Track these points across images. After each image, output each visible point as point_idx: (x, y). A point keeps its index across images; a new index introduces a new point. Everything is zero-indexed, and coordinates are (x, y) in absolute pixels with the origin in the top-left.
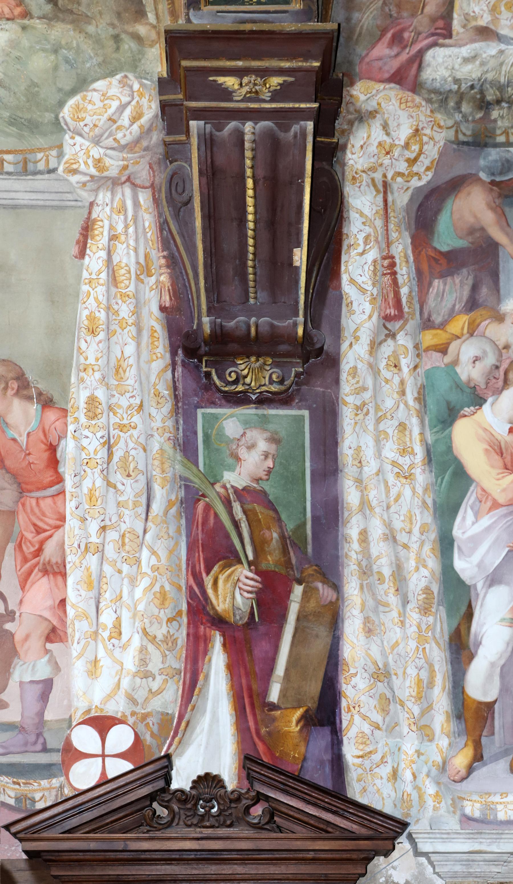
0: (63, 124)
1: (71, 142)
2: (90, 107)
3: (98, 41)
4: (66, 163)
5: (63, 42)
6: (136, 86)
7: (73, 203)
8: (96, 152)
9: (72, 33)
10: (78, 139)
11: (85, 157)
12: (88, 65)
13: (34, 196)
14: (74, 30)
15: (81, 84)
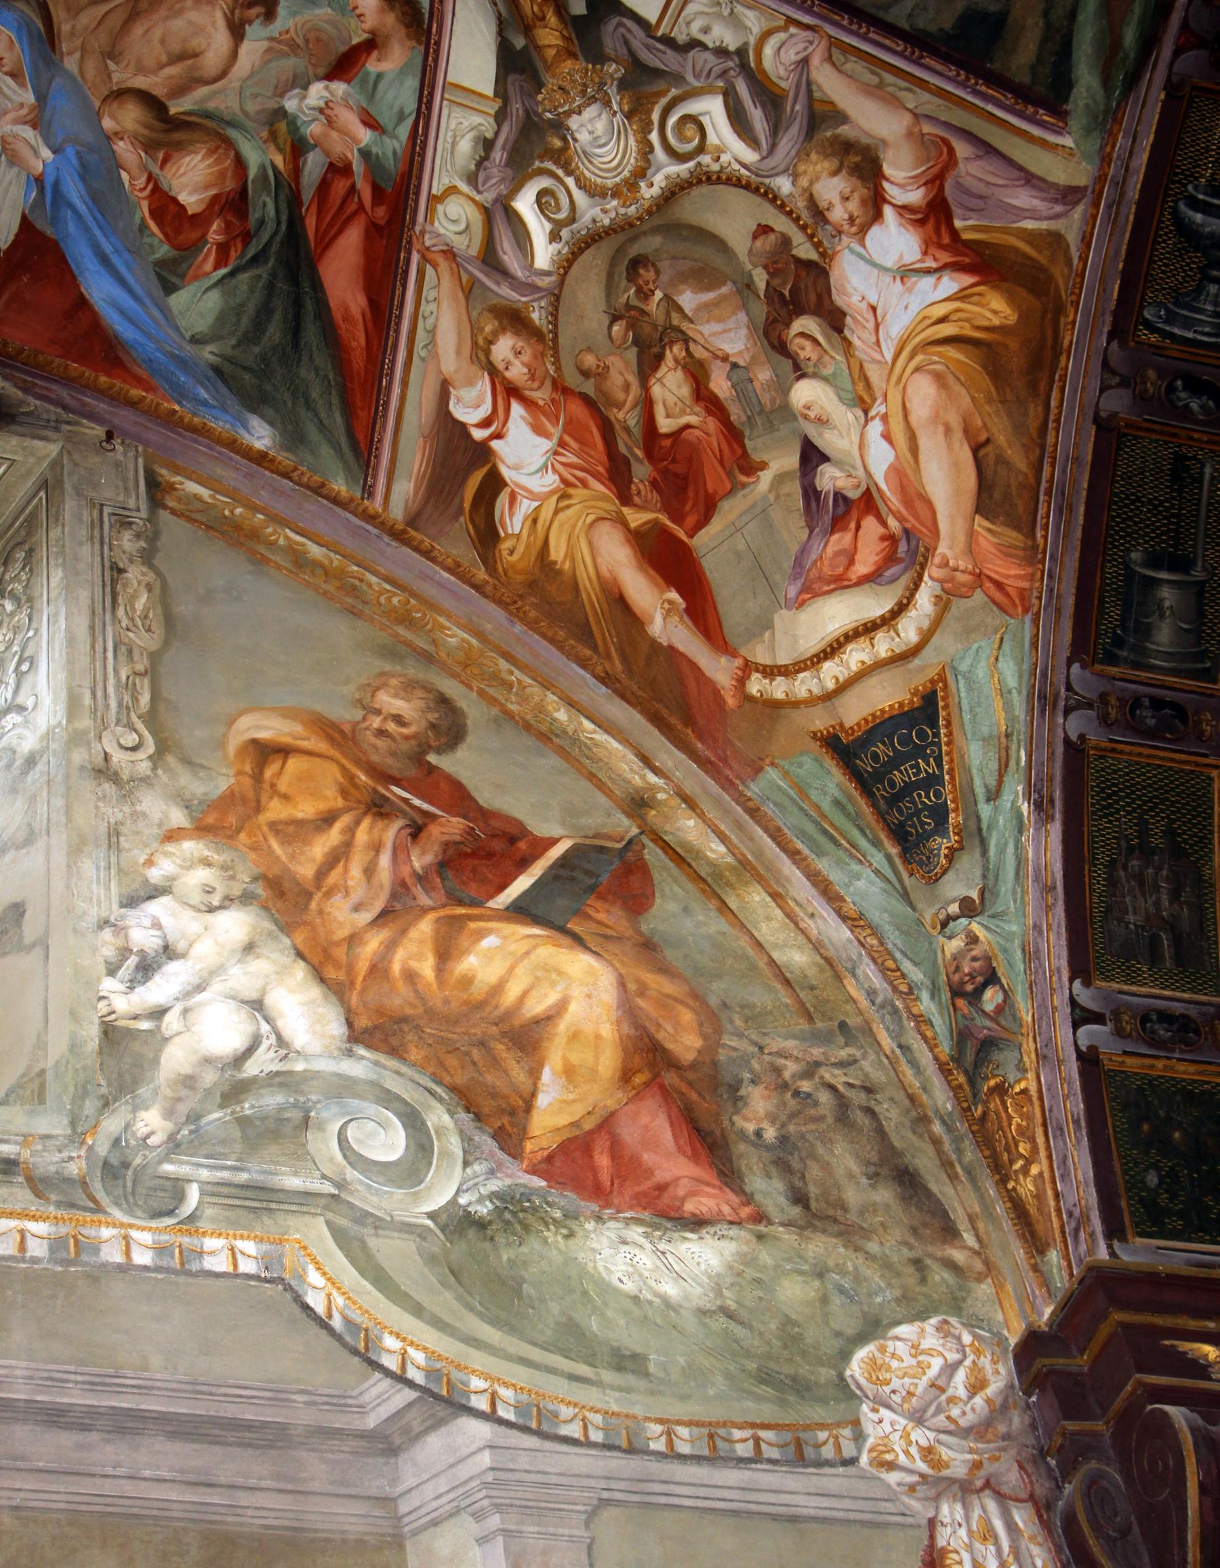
0: (853, 1387)
1: (875, 1417)
2: (895, 1364)
3: (887, 1265)
4: (871, 1451)
5: (831, 1263)
6: (967, 1338)
7: (900, 1519)
8: (921, 1436)
9: (842, 1250)
10: (884, 1412)
11: (903, 1443)
12: (879, 1300)
13: (826, 1503)
14: (845, 1246)
15: (873, 1328)
